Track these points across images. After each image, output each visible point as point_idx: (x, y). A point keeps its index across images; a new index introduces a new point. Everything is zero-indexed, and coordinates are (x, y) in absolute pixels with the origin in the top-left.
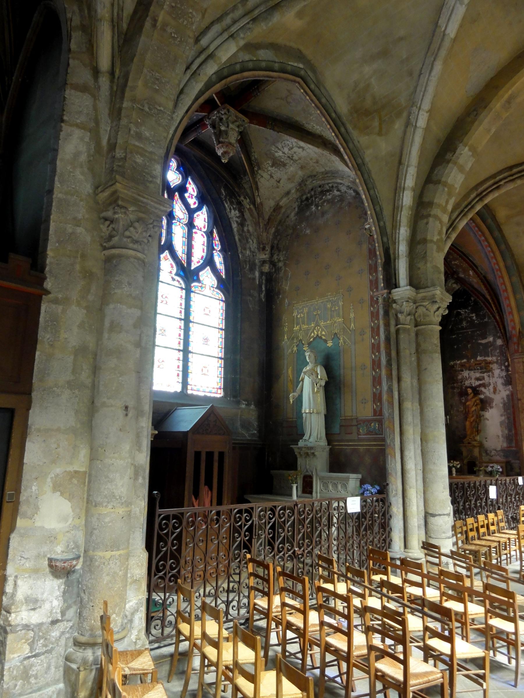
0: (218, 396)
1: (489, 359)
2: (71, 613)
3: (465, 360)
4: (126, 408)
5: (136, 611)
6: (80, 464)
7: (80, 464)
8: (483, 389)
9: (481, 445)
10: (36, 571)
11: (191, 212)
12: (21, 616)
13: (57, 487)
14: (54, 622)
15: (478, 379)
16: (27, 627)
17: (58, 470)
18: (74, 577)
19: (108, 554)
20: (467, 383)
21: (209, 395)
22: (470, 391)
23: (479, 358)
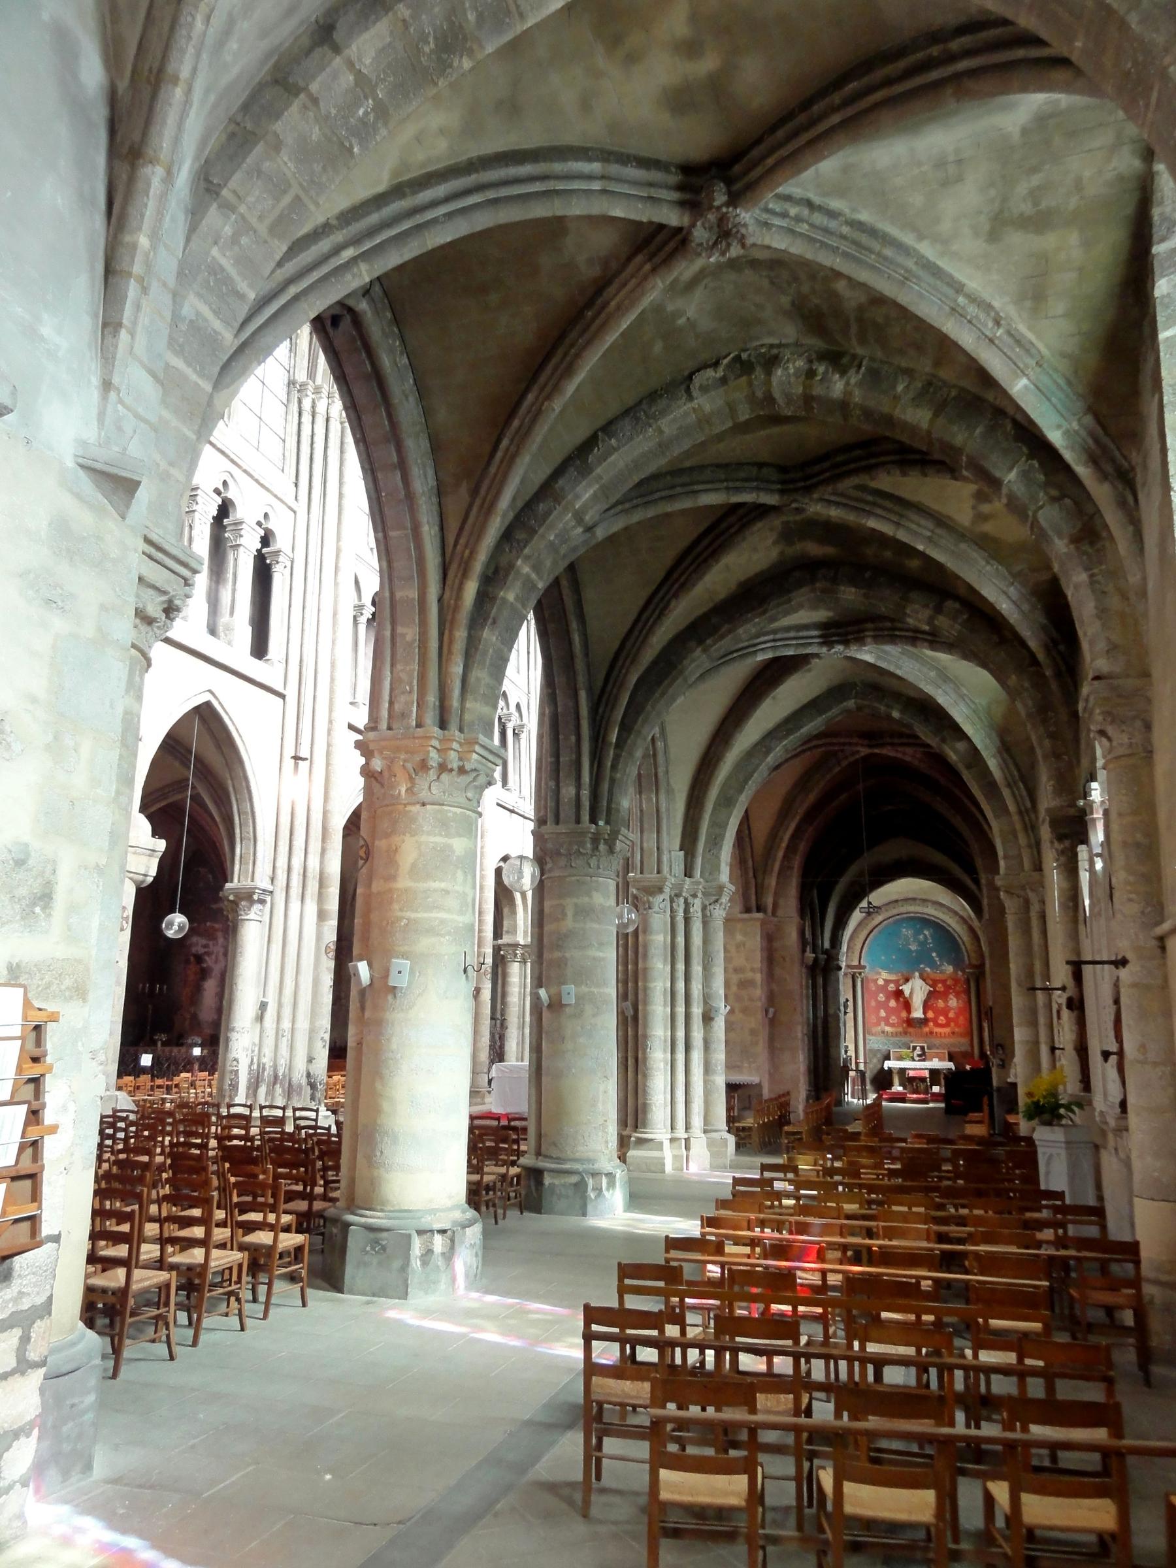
1: (217, 926)
8: (207, 958)
9: (194, 1017)
15: (205, 946)
20: (194, 950)
22: (192, 959)
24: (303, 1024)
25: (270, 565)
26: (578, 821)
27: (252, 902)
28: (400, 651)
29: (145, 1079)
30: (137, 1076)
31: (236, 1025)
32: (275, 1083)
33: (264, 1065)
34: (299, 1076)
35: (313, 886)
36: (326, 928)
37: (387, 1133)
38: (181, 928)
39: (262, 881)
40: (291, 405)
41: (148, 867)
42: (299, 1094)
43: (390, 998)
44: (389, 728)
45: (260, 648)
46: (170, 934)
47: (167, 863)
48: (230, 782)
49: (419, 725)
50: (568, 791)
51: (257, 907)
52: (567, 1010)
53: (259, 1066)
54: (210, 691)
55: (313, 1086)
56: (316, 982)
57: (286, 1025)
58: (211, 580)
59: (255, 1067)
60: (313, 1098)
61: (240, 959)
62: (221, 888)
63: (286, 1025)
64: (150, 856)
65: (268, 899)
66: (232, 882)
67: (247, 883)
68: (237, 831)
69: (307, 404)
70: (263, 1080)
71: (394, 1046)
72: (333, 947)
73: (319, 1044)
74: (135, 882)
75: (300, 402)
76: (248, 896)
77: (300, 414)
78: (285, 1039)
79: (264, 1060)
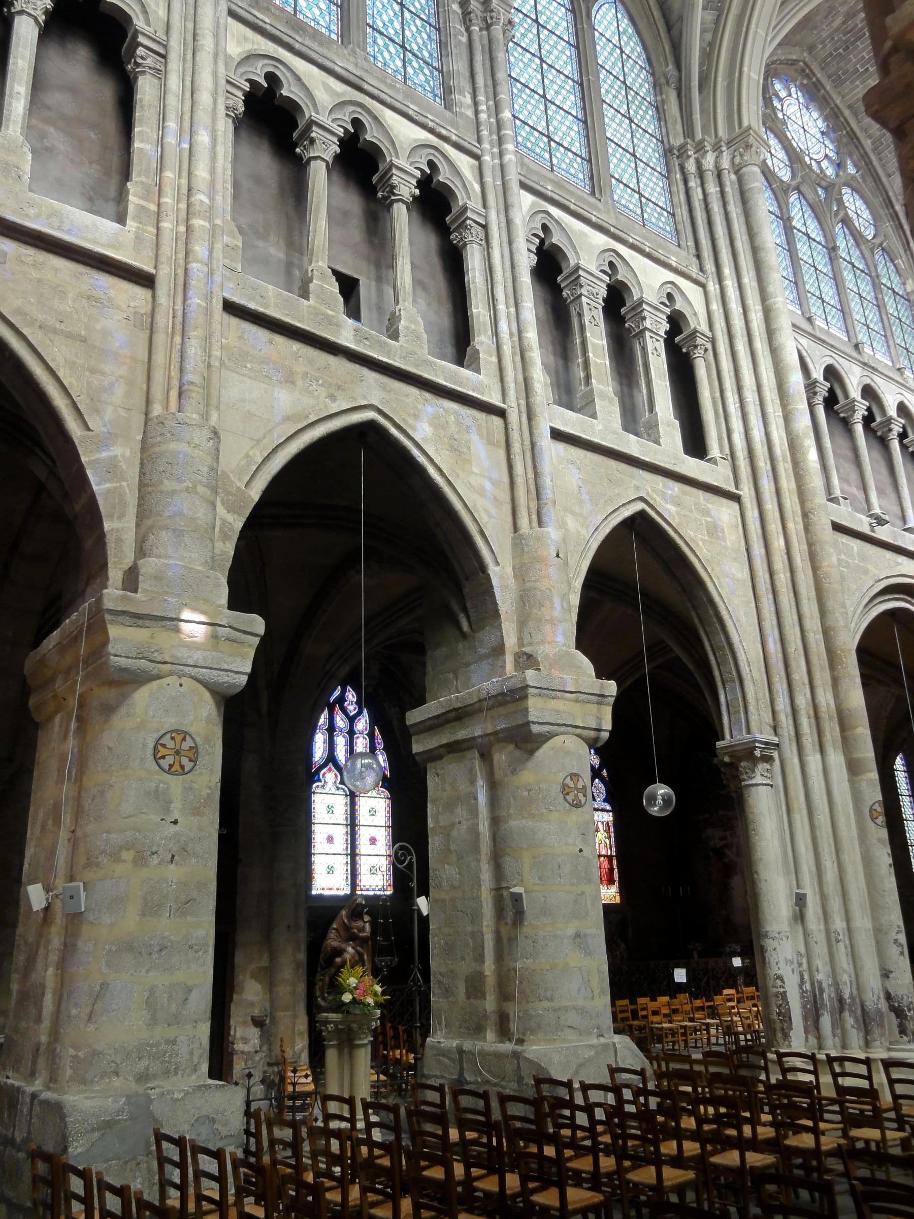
0: (388, 893)
2: (265, 1048)
3: (707, 815)
4: (289, 927)
5: (302, 1051)
6: (265, 963)
7: (265, 963)
8: (726, 851)
10: (245, 1023)
11: (352, 720)
12: (239, 1046)
13: (252, 977)
14: (256, 1052)
15: (722, 838)
16: (243, 1052)
17: (253, 966)
18: (265, 1028)
19: (283, 1014)
21: (378, 893)
22: (711, 854)
23: (721, 813)
24: (862, 922)
25: (688, 353)
27: (755, 761)
29: (683, 997)
30: (673, 996)
31: (768, 929)
32: (841, 1011)
33: (820, 983)
34: (874, 997)
35: (832, 730)
36: (864, 784)
38: (667, 801)
39: (763, 734)
40: (673, 175)
41: (599, 719)
42: (881, 1025)
45: (695, 443)
46: (655, 810)
47: (622, 709)
48: (693, 613)
51: (762, 767)
53: (812, 984)
54: (642, 499)
56: (868, 861)
57: (839, 924)
58: (621, 384)
59: (808, 986)
61: (755, 839)
62: (713, 750)
63: (839, 924)
64: (599, 703)
65: (775, 754)
66: (723, 739)
67: (742, 737)
68: (716, 673)
69: (691, 166)
70: (823, 1005)
72: (879, 809)
73: (894, 951)
74: (586, 740)
76: (748, 754)
77: (686, 182)
78: (841, 945)
79: (820, 977)
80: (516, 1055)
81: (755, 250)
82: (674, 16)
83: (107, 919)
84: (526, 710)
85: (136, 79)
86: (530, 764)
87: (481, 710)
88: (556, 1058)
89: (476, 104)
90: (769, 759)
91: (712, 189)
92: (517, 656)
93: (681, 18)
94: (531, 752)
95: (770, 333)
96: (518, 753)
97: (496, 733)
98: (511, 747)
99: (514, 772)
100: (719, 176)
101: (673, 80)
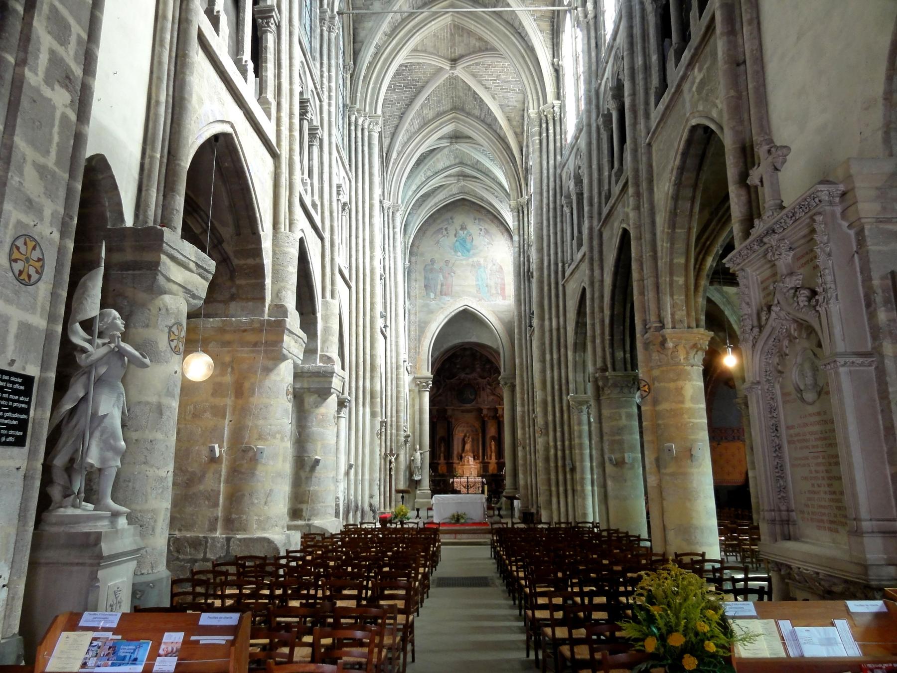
24: (367, 477)
26: (626, 370)
28: (675, 289)
37: (697, 528)
43: (689, 461)
44: (674, 328)
49: (689, 327)
50: (619, 355)
51: (344, 409)
52: (627, 466)
53: (348, 501)
55: (374, 512)
57: (360, 477)
60: (374, 518)
69: (353, 118)
71: (695, 485)
75: (349, 117)
77: (350, 125)
79: (352, 497)
80: (309, 526)
81: (371, 174)
82: (359, 39)
83: (271, 463)
84: (331, 382)
85: (266, 31)
86: (324, 405)
87: (301, 376)
88: (329, 525)
89: (322, 71)
90: (346, 407)
91: (359, 135)
92: (322, 356)
93: (362, 42)
94: (325, 399)
95: (371, 217)
96: (319, 399)
97: (309, 389)
98: (316, 396)
99: (317, 407)
100: (363, 130)
101: (352, 70)
